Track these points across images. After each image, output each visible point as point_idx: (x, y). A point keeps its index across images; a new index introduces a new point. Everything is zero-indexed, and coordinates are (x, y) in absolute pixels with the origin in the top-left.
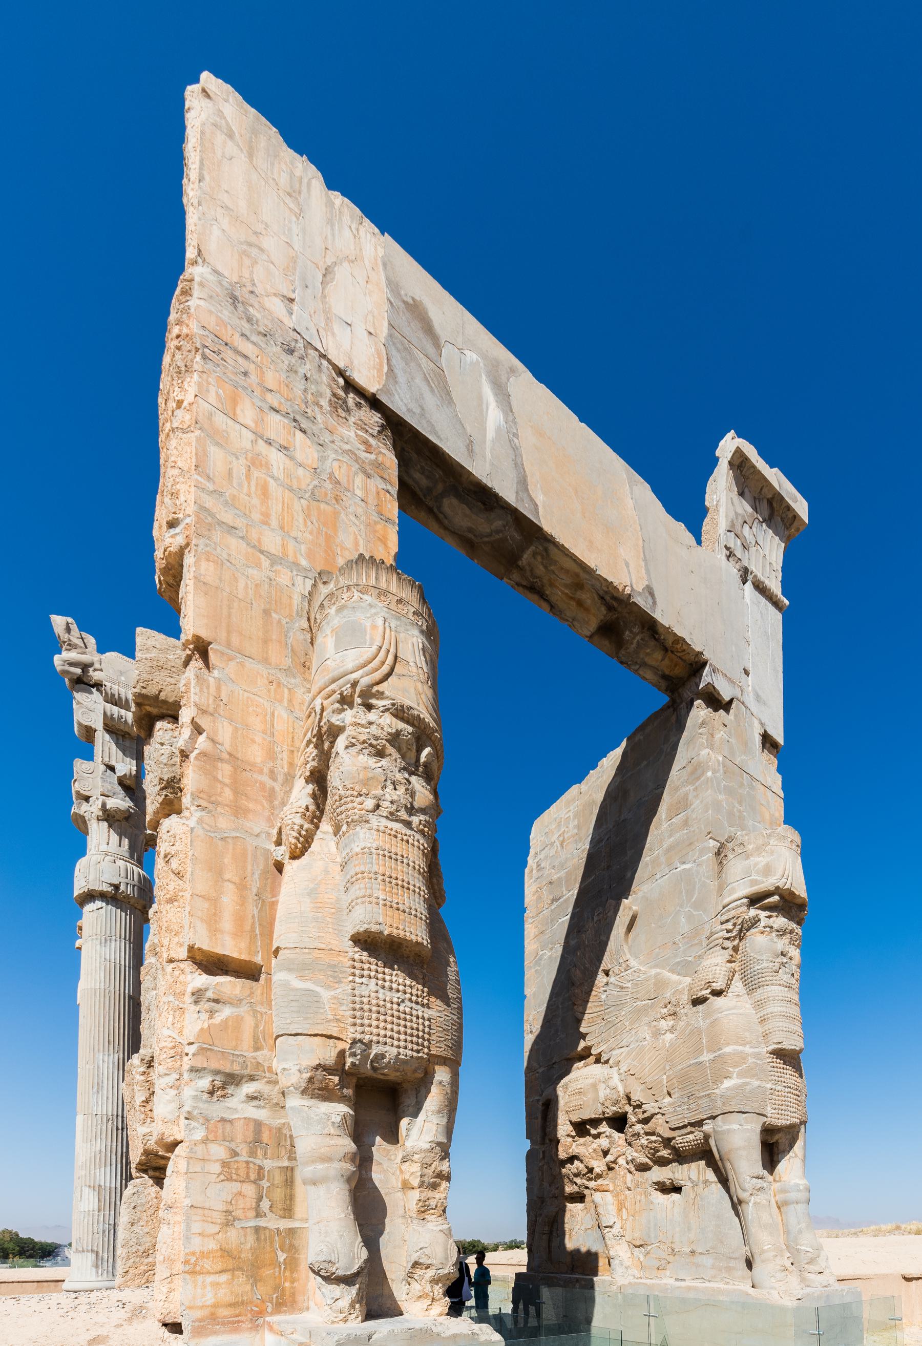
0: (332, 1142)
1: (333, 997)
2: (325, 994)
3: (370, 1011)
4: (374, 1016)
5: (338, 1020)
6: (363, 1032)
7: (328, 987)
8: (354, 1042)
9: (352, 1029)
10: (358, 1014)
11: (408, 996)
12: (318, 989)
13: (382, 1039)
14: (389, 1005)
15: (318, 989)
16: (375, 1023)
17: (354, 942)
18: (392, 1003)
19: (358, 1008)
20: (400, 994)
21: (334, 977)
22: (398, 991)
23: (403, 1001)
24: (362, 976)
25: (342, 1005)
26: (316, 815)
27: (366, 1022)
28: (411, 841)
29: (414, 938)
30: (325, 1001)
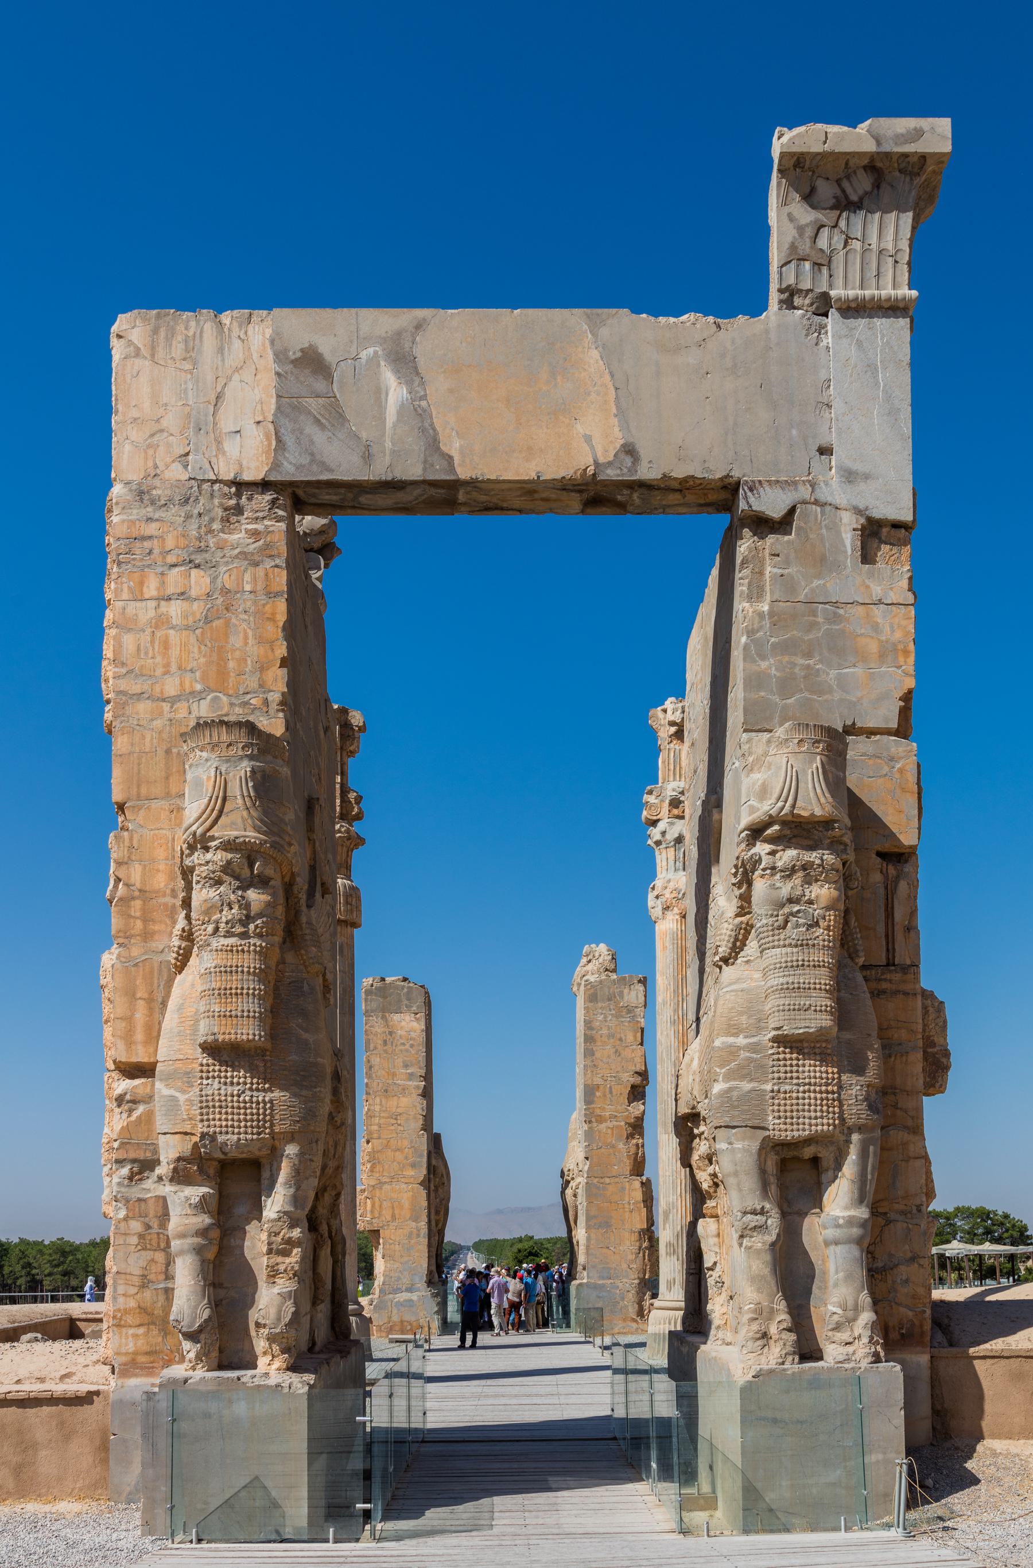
0: (187, 1222)
1: (187, 1100)
2: (182, 1098)
3: (214, 1107)
4: (217, 1110)
5: (190, 1119)
6: (209, 1126)
7: (183, 1092)
8: (203, 1136)
9: (200, 1126)
10: (204, 1111)
11: (248, 1086)
12: (178, 1094)
13: (224, 1129)
14: (229, 1099)
15: (178, 1094)
16: (218, 1116)
17: (203, 1049)
18: (233, 1096)
19: (206, 1106)
20: (239, 1087)
21: (188, 1082)
22: (238, 1084)
23: (243, 1092)
24: (208, 1078)
25: (193, 1105)
26: (188, 936)
27: (211, 1117)
28: (246, 949)
29: (244, 1037)
30: (181, 1103)
